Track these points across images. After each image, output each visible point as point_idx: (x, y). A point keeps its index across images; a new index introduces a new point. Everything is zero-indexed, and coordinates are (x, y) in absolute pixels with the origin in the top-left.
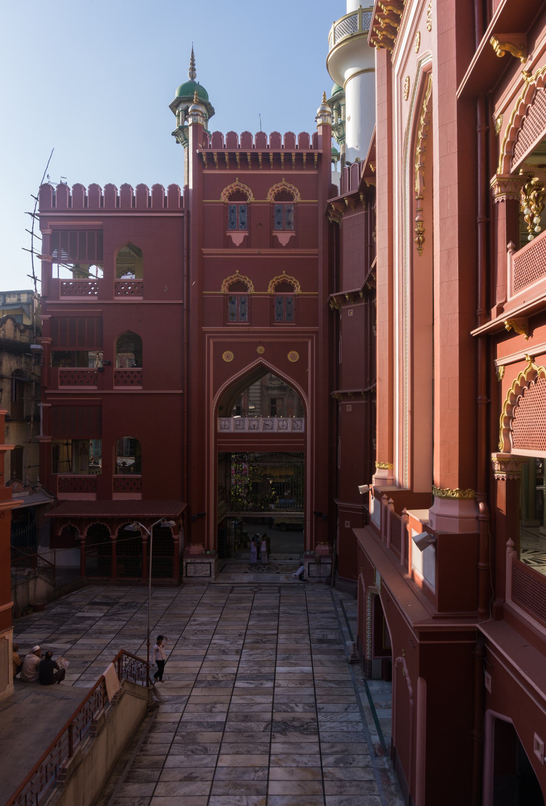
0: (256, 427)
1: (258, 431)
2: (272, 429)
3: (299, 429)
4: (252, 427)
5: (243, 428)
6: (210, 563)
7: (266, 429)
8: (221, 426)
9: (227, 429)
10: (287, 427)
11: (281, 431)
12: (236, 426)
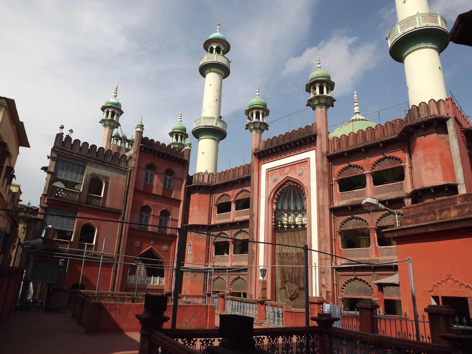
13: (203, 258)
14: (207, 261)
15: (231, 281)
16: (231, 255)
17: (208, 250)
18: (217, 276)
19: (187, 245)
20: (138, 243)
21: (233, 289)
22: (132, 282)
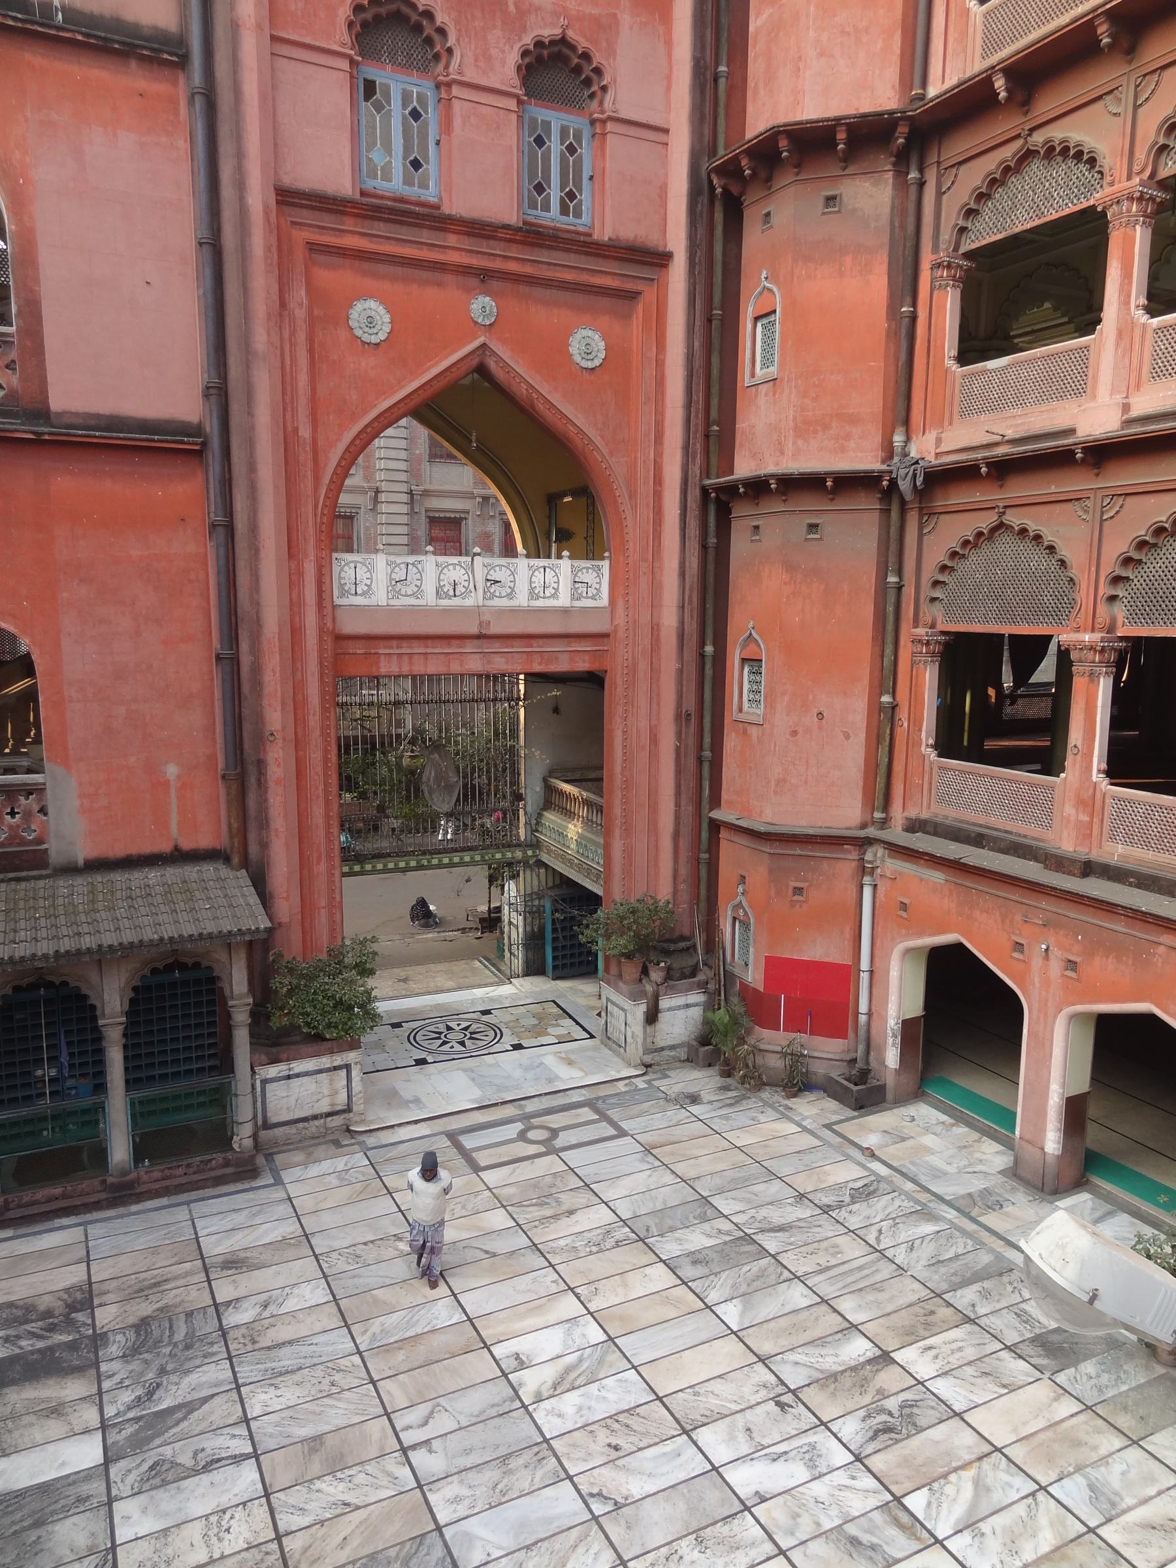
0: (460, 589)
1: (469, 602)
2: (510, 596)
3: (593, 598)
4: (448, 588)
5: (418, 593)
6: (348, 1067)
7: (493, 596)
8: (342, 586)
9: (364, 594)
10: (557, 590)
11: (540, 603)
12: (395, 584)
13: (869, 398)
14: (901, 412)
15: (1118, 545)
16: (1125, 331)
17: (905, 332)
18: (985, 522)
19: (748, 311)
20: (370, 317)
21: (1133, 617)
22: (380, 597)
